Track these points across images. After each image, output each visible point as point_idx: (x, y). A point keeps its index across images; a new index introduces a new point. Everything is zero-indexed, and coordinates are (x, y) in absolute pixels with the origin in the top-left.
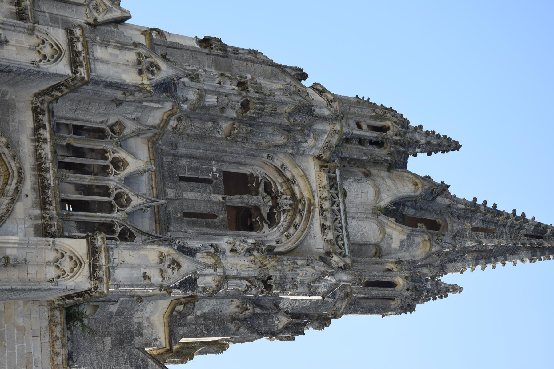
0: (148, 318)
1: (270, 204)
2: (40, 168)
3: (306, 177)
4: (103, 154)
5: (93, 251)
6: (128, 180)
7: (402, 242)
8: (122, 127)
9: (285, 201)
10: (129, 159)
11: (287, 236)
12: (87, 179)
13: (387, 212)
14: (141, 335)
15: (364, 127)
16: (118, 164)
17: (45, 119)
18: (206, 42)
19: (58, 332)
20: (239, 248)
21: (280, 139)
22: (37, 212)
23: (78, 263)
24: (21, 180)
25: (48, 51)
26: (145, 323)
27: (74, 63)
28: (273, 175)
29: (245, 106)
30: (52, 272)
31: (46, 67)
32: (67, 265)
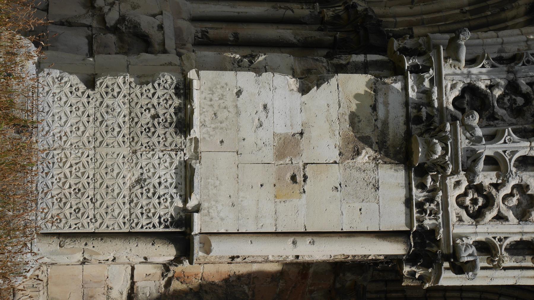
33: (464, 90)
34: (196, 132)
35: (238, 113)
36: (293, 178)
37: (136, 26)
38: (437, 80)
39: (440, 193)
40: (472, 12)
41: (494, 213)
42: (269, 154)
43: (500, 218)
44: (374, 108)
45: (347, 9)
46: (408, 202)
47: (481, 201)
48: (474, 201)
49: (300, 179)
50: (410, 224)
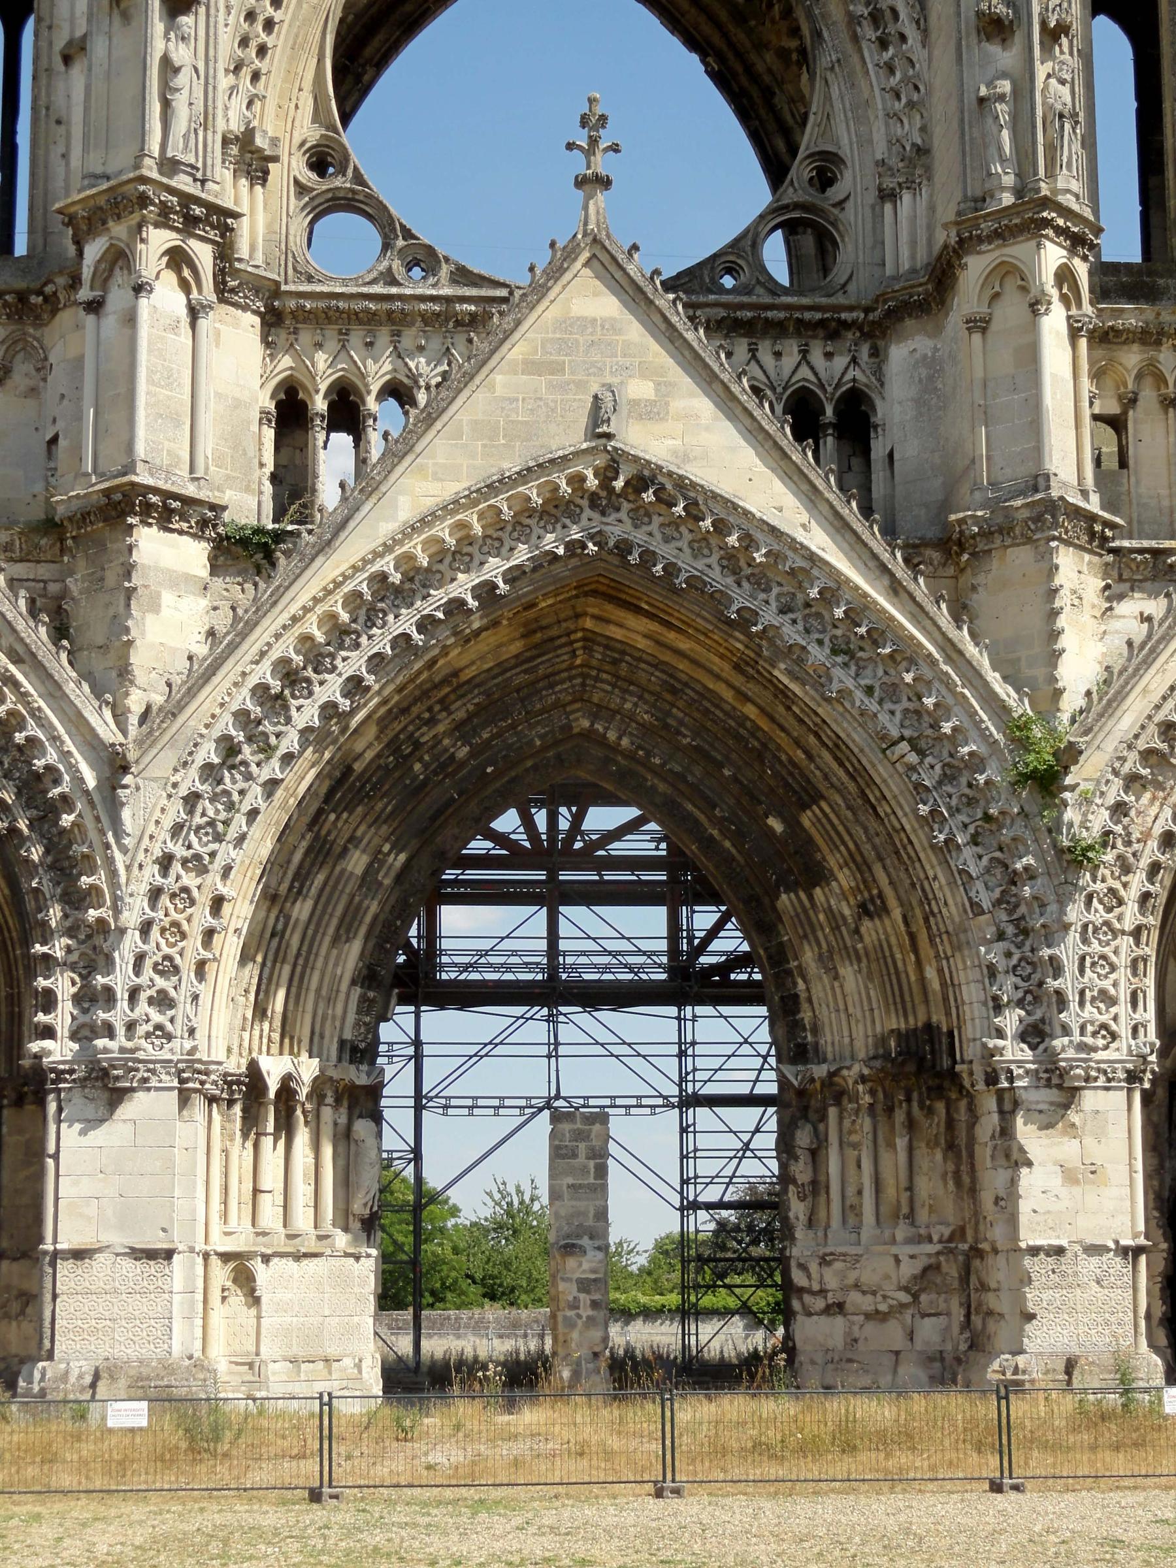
33: (1024, 1041)
34: (1064, 1242)
35: (1049, 1212)
36: (1093, 1173)
37: (915, 1277)
38: (1020, 1063)
39: (1102, 1066)
40: (859, 960)
41: (1112, 1023)
42: (1077, 1190)
43: (1115, 1019)
44: (1040, 1112)
45: (863, 1082)
46: (1107, 1089)
47: (1103, 1032)
48: (1104, 1037)
49: (1093, 1168)
50: (1121, 1088)
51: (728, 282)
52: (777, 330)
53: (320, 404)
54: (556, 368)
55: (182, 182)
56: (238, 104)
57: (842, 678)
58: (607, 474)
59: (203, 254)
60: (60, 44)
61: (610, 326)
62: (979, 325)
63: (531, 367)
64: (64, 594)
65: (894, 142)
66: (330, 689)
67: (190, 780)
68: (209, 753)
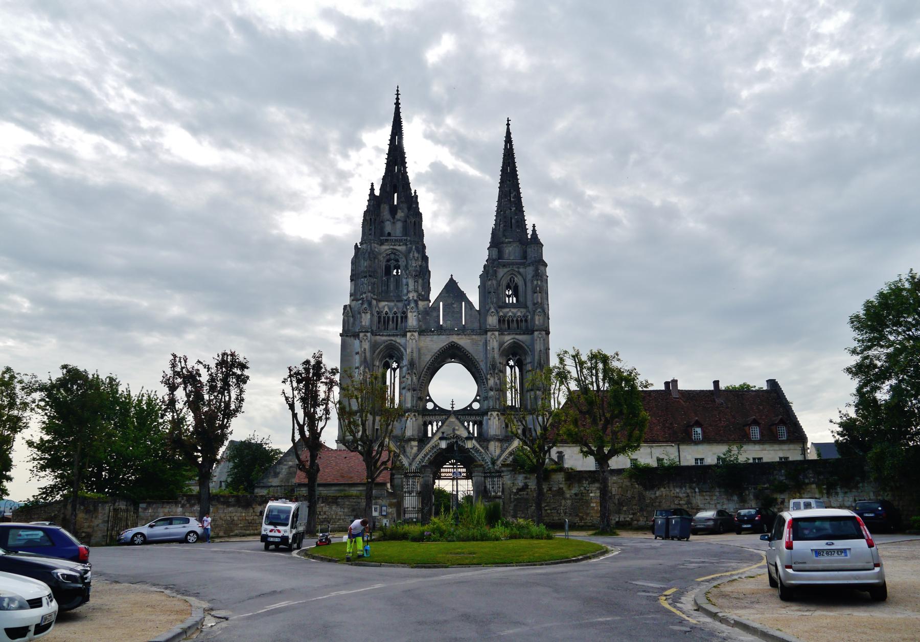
0: (423, 306)
1: (393, 261)
2: (389, 335)
3: (386, 250)
4: (384, 317)
5: (410, 331)
6: (390, 309)
7: (402, 212)
8: (377, 311)
9: (392, 256)
10: (385, 311)
11: (402, 258)
12: (391, 323)
13: (394, 218)
14: (426, 308)
15: (371, 227)
16: (386, 313)
17: (378, 334)
18: (352, 280)
19: (426, 334)
20: (406, 277)
21: (376, 260)
22: (399, 337)
23: (412, 335)
24: (392, 340)
25: (365, 338)
26: (424, 307)
27: (368, 332)
28: (385, 260)
29: (370, 276)
30: (414, 341)
31: (369, 339)
32: (412, 337)
51: (469, 408)
52: (473, 415)
53: (428, 423)
54: (449, 426)
55: (415, 408)
56: (419, 394)
57: (475, 454)
58: (454, 436)
59: (417, 414)
60: (402, 387)
61: (454, 422)
62: (490, 419)
63: (447, 426)
64: (404, 447)
65: (485, 395)
66: (429, 456)
67: (416, 465)
68: (418, 463)
